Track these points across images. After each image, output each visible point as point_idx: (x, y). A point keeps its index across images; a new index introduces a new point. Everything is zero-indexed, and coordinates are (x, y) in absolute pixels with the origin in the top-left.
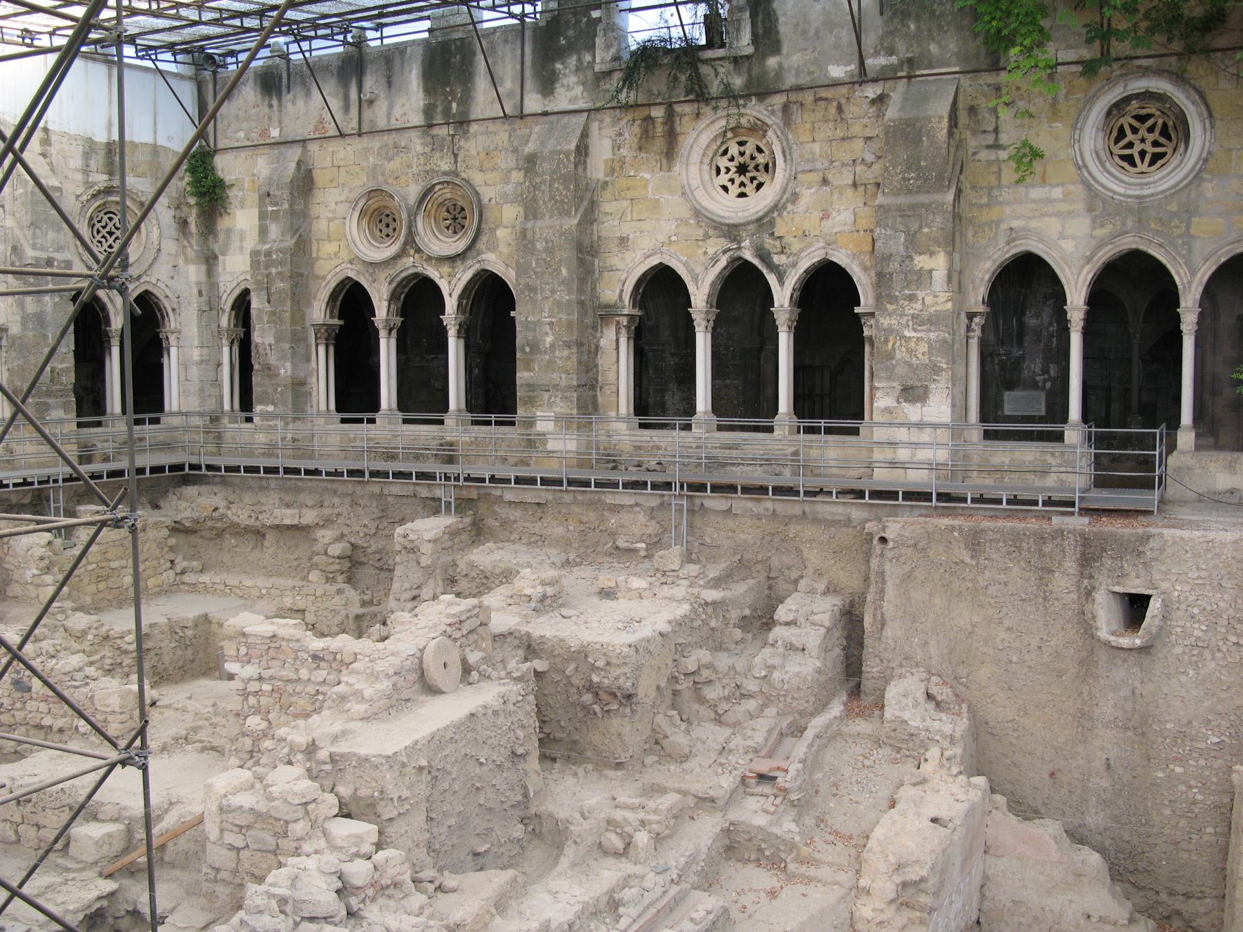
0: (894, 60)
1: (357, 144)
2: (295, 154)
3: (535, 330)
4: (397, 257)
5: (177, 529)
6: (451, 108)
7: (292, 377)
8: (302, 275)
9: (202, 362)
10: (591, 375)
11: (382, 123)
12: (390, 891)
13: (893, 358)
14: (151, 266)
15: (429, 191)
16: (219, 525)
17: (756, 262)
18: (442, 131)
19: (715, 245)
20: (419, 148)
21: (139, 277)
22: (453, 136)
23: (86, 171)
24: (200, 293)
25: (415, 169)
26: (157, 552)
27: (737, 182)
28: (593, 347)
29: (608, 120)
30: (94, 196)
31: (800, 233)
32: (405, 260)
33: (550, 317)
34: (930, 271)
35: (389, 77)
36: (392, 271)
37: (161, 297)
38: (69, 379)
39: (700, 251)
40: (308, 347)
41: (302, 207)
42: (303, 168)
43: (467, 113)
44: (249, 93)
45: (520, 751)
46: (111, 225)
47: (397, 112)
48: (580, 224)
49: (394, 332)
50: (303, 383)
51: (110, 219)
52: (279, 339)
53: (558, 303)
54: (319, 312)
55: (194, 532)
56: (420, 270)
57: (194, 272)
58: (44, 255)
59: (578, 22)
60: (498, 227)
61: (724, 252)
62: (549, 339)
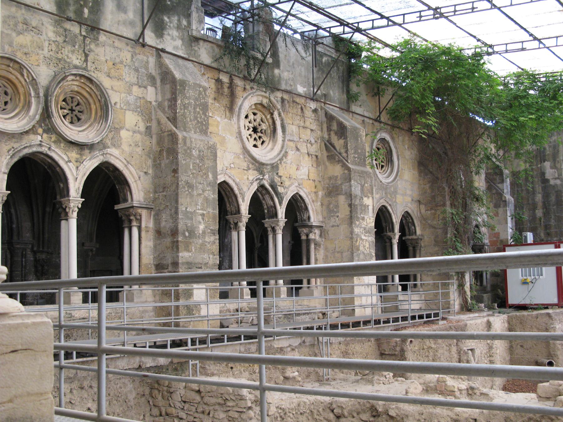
3: (192, 219)
6: (82, 12)
13: (359, 250)
17: (270, 189)
19: (253, 175)
20: (51, 35)
22: (85, 37)
27: (253, 138)
31: (288, 176)
32: (32, 137)
33: (202, 209)
34: (368, 206)
39: (246, 177)
43: (98, 22)
53: (206, 199)
56: (44, 149)
60: (122, 128)
61: (256, 180)
62: (202, 227)
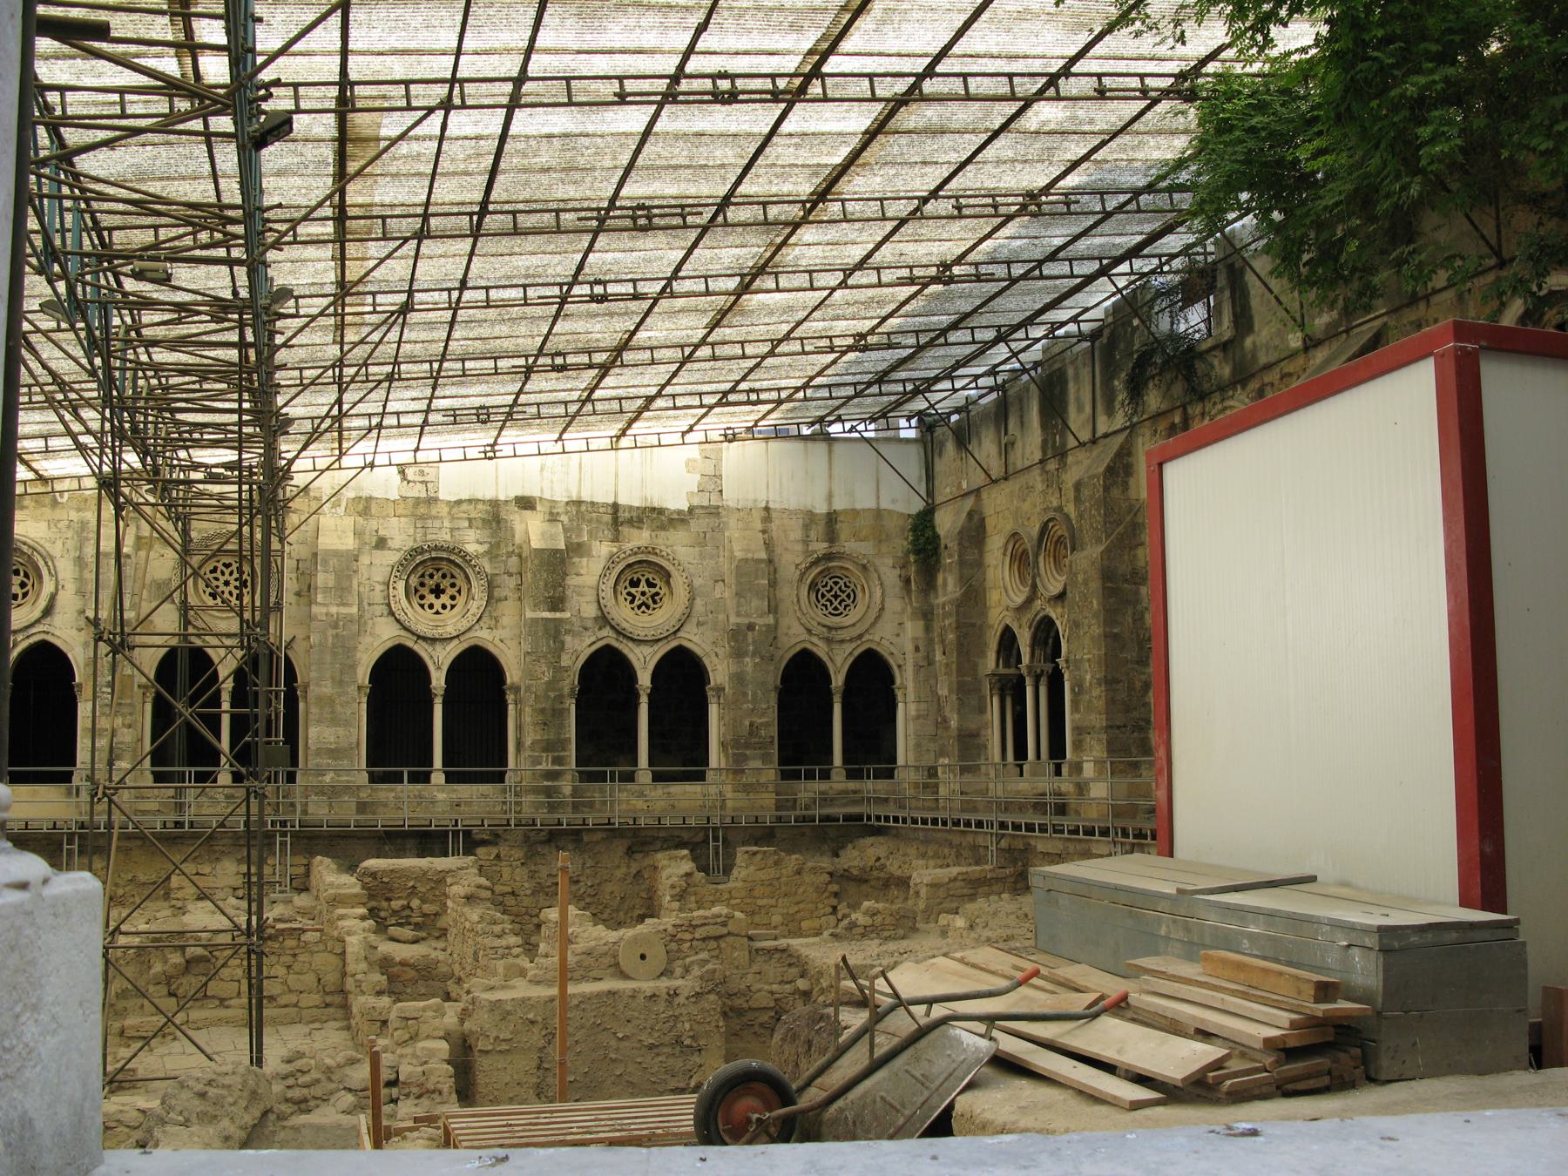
0: (1335, 314)
1: (1007, 487)
2: (969, 503)
4: (1029, 601)
5: (843, 877)
7: (959, 729)
8: (973, 625)
9: (918, 717)
10: (1135, 714)
11: (1019, 466)
12: (436, 1096)
14: (873, 624)
15: (1044, 529)
16: (882, 875)
18: (1052, 465)
21: (860, 636)
23: (806, 541)
24: (917, 649)
25: (1038, 509)
26: (815, 895)
28: (1138, 685)
29: (1148, 433)
30: (814, 564)
35: (1022, 417)
36: (1029, 616)
37: (886, 655)
38: (774, 731)
40: (982, 699)
41: (976, 556)
42: (976, 517)
44: (950, 447)
45: (688, 1042)
46: (836, 588)
47: (1028, 452)
48: (1108, 550)
49: (1044, 681)
50: (975, 735)
51: (836, 583)
52: (950, 691)
54: (990, 662)
55: (866, 881)
57: (913, 629)
58: (746, 621)
59: (1126, 332)
62: (1088, 677)
